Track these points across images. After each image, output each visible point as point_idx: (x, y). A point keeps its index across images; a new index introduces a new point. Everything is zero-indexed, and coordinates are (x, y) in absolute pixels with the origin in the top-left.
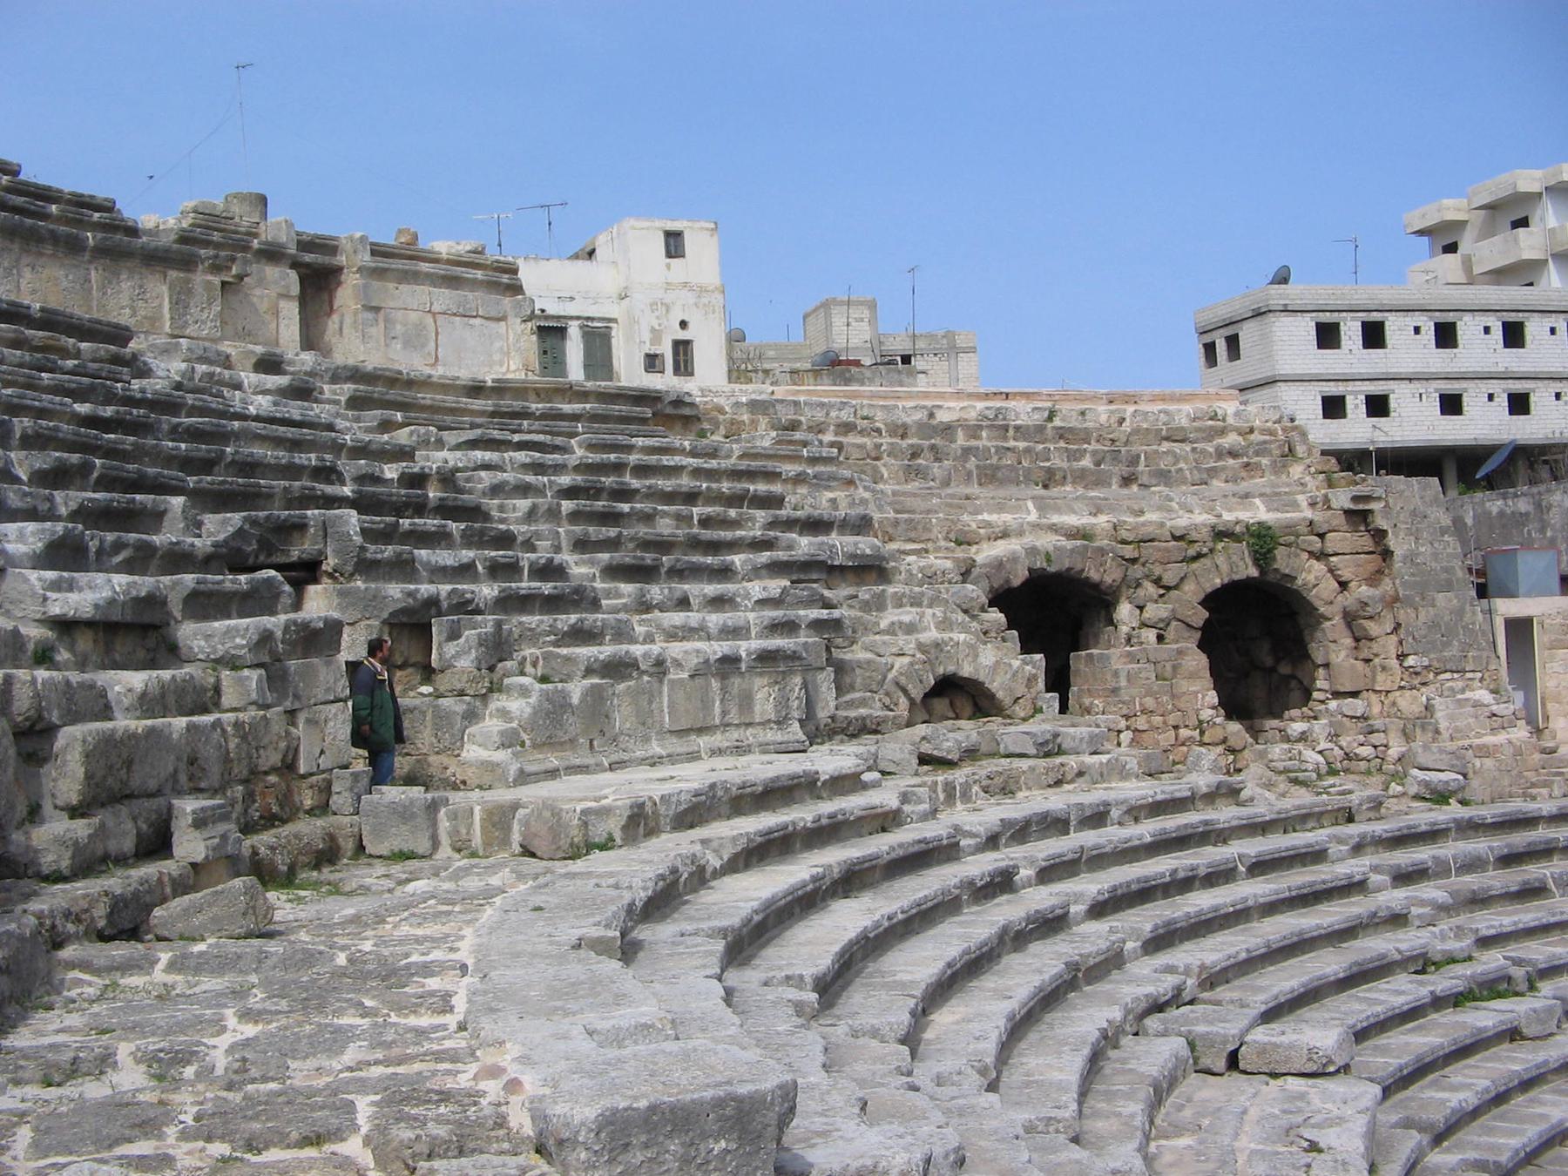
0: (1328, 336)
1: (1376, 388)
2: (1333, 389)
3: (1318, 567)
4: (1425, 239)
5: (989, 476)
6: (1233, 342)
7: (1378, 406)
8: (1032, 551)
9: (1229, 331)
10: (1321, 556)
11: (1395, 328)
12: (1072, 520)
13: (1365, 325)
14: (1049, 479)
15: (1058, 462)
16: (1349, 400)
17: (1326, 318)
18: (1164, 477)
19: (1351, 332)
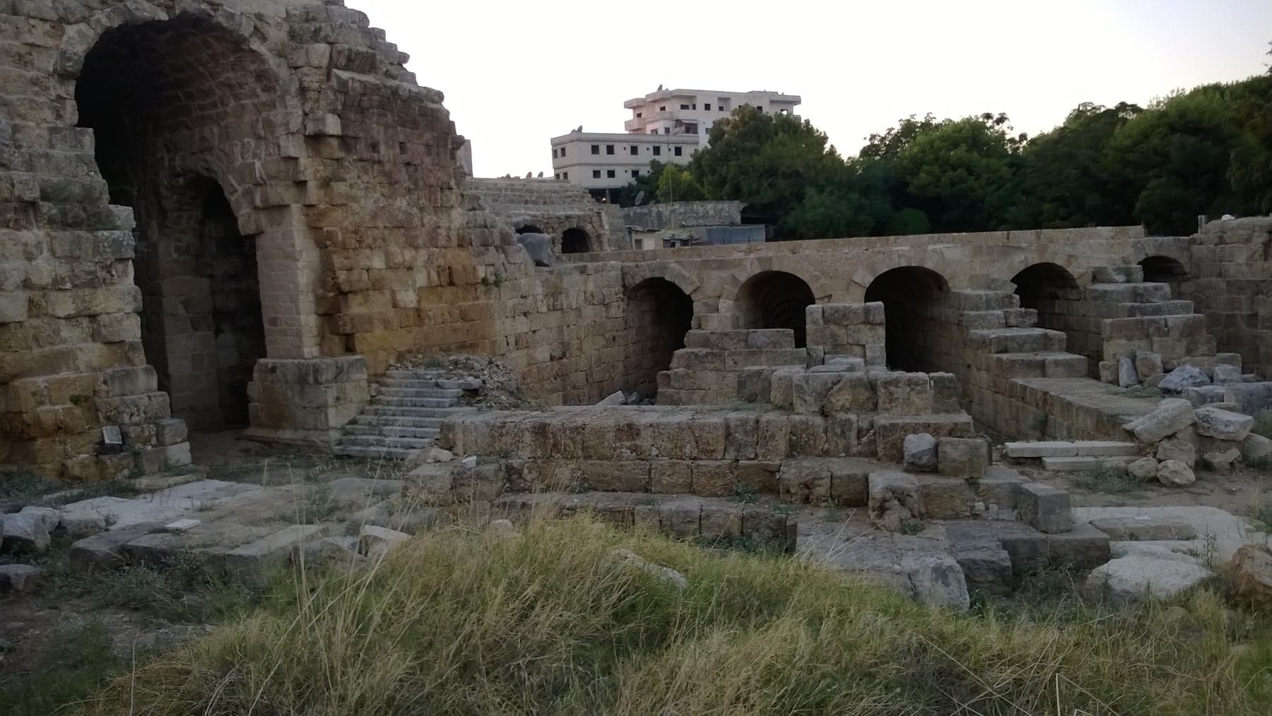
0: (595, 150)
1: (611, 168)
2: (597, 168)
3: (590, 226)
4: (631, 110)
5: (511, 201)
6: (563, 150)
7: (611, 174)
8: (525, 220)
9: (562, 146)
10: (591, 223)
11: (618, 148)
12: (532, 213)
13: (608, 147)
14: (526, 202)
15: (528, 198)
16: (602, 173)
17: (595, 144)
18: (552, 203)
19: (603, 149)
